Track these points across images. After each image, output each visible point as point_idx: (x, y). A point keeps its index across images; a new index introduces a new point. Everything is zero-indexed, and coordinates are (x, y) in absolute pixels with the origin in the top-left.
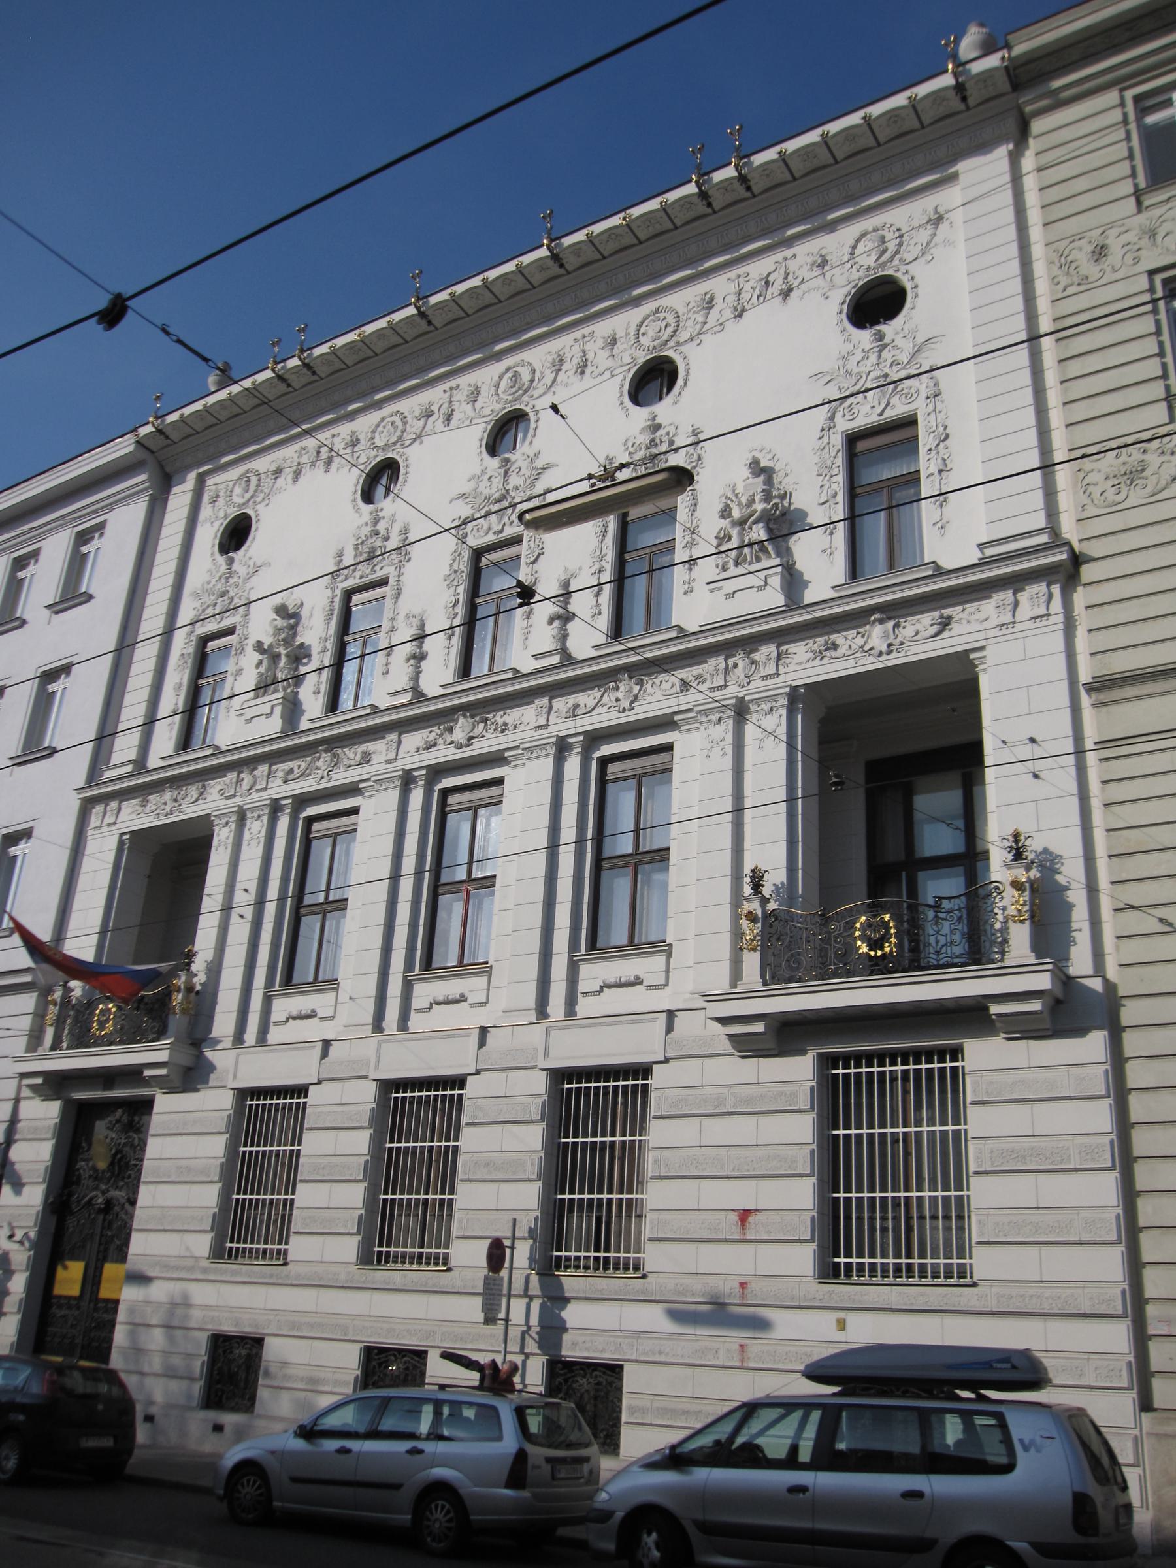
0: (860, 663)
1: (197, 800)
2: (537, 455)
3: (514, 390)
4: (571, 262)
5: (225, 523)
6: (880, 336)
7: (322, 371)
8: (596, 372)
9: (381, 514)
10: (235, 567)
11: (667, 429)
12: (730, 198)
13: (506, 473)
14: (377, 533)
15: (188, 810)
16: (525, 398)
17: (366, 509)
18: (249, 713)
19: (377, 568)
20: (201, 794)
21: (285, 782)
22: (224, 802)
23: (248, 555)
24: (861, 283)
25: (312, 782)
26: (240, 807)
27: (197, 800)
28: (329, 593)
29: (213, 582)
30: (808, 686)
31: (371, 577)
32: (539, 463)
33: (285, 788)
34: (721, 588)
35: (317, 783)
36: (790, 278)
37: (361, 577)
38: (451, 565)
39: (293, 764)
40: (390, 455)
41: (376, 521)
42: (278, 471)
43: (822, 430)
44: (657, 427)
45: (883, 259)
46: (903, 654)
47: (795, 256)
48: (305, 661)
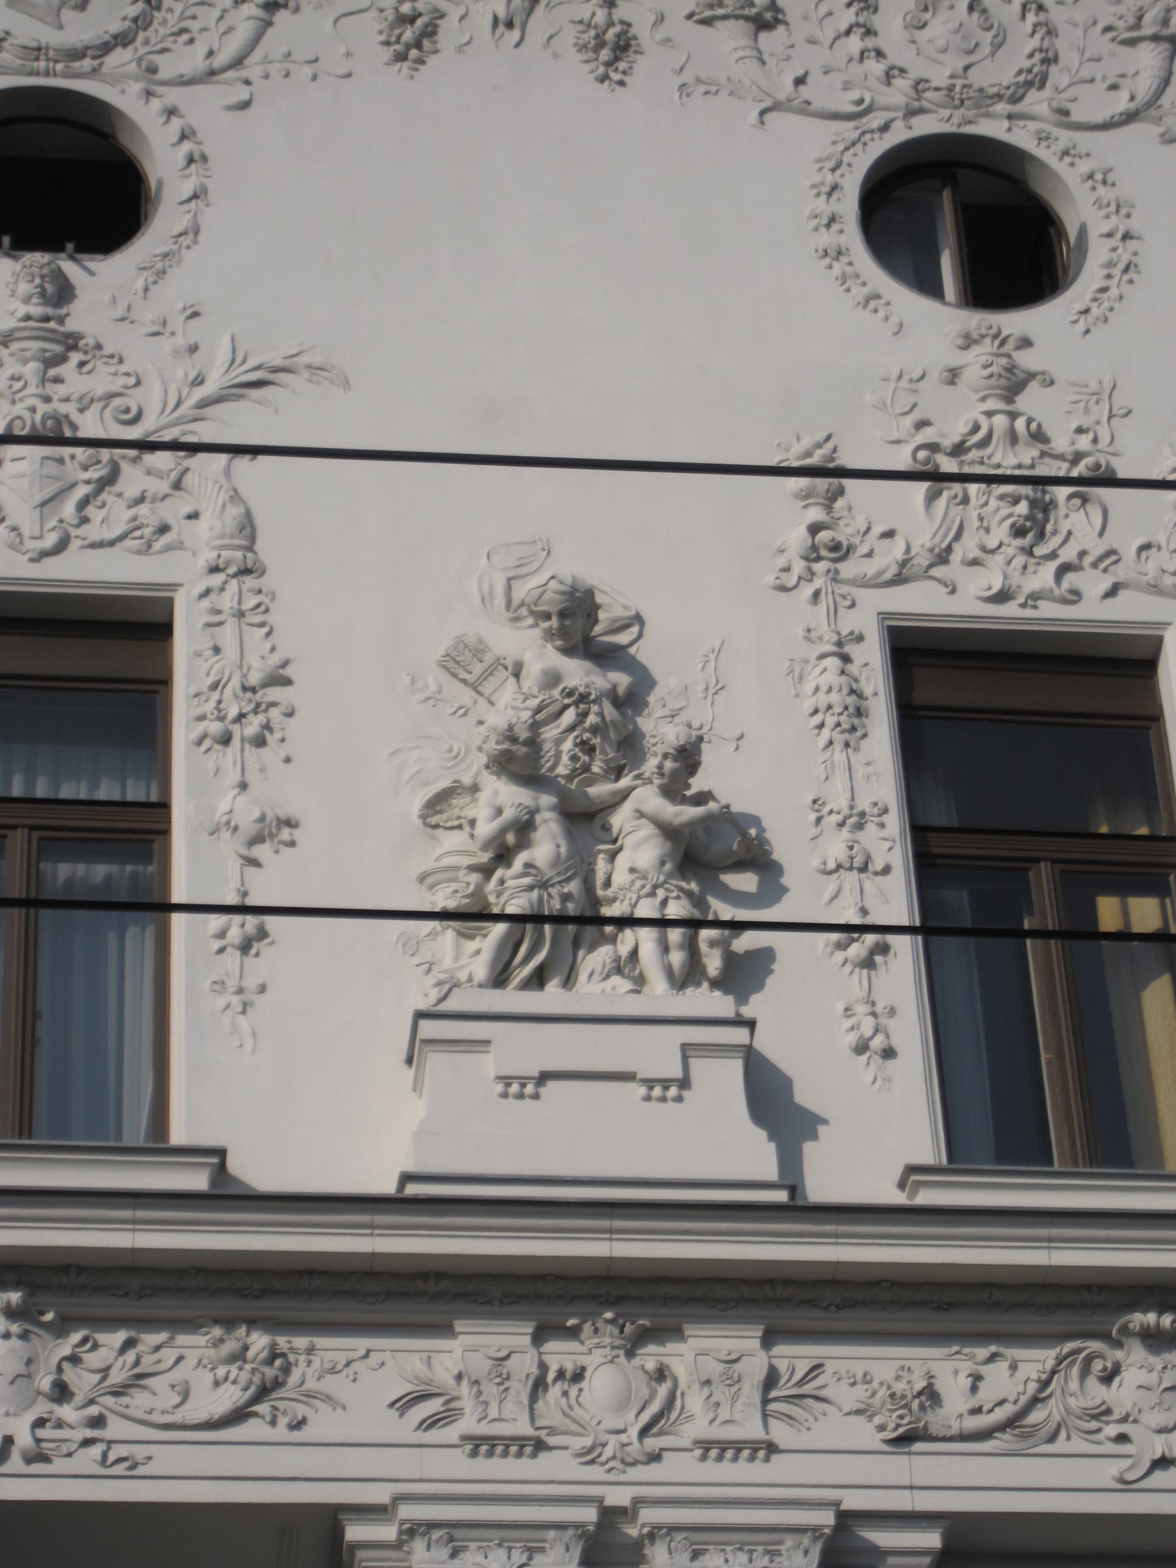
1: (238, 1416)
9: (1027, 360)
10: (81, 317)
14: (1039, 436)
15: (169, 1459)
19: (1093, 583)
20: (264, 1392)
21: (904, 1440)
22: (457, 1464)
23: (174, 293)
25: (1114, 1468)
27: (238, 1416)
31: (1048, 610)
33: (897, 1467)
35: (1125, 1484)
37: (1002, 597)
39: (949, 1369)
40: (993, 128)
41: (1013, 384)
48: (745, 882)
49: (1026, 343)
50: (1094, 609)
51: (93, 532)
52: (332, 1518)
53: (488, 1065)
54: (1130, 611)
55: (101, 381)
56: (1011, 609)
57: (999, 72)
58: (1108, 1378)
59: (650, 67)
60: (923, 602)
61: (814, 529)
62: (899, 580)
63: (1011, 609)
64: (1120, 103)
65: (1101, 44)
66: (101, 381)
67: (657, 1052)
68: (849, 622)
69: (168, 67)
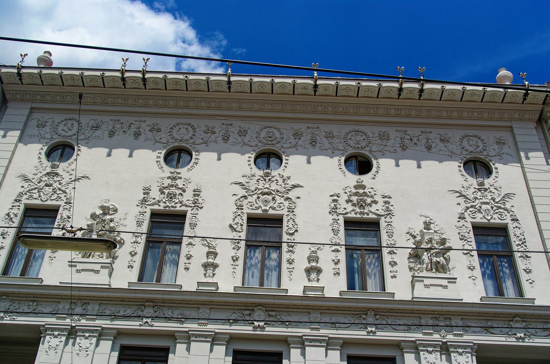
0: (509, 340)
2: (289, 178)
3: (268, 139)
4: (320, 91)
5: (51, 143)
6: (482, 184)
7: (149, 85)
8: (323, 147)
10: (59, 171)
11: (370, 190)
12: (410, 96)
13: (270, 180)
16: (279, 145)
17: (168, 170)
18: (80, 267)
24: (468, 157)
26: (73, 327)
28: (139, 209)
29: (41, 175)
30: (479, 345)
32: (291, 182)
34: (423, 281)
36: (430, 141)
38: (234, 220)
42: (96, 128)
43: (459, 218)
44: (364, 187)
45: (478, 150)
46: (531, 341)
47: (430, 132)
49: (179, 173)
50: (179, 208)
51: (52, 198)
52: (39, 326)
53: (74, 269)
54: (184, 208)
55: (59, 179)
56: (167, 209)
57: (188, 137)
58: (142, 311)
59: (142, 137)
60: (156, 207)
61: (144, 198)
62: (153, 205)
63: (167, 209)
64: (202, 141)
65: (202, 133)
66: (59, 179)
67: (97, 267)
68: (145, 210)
69: (80, 138)
